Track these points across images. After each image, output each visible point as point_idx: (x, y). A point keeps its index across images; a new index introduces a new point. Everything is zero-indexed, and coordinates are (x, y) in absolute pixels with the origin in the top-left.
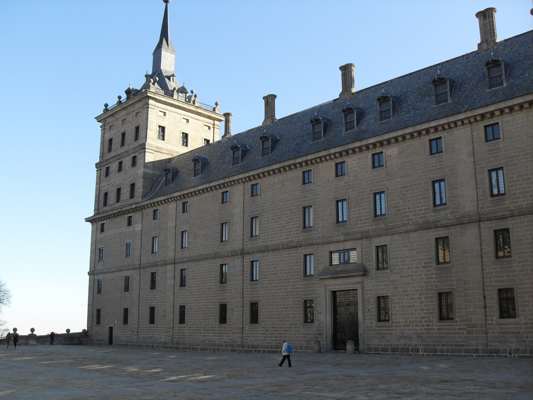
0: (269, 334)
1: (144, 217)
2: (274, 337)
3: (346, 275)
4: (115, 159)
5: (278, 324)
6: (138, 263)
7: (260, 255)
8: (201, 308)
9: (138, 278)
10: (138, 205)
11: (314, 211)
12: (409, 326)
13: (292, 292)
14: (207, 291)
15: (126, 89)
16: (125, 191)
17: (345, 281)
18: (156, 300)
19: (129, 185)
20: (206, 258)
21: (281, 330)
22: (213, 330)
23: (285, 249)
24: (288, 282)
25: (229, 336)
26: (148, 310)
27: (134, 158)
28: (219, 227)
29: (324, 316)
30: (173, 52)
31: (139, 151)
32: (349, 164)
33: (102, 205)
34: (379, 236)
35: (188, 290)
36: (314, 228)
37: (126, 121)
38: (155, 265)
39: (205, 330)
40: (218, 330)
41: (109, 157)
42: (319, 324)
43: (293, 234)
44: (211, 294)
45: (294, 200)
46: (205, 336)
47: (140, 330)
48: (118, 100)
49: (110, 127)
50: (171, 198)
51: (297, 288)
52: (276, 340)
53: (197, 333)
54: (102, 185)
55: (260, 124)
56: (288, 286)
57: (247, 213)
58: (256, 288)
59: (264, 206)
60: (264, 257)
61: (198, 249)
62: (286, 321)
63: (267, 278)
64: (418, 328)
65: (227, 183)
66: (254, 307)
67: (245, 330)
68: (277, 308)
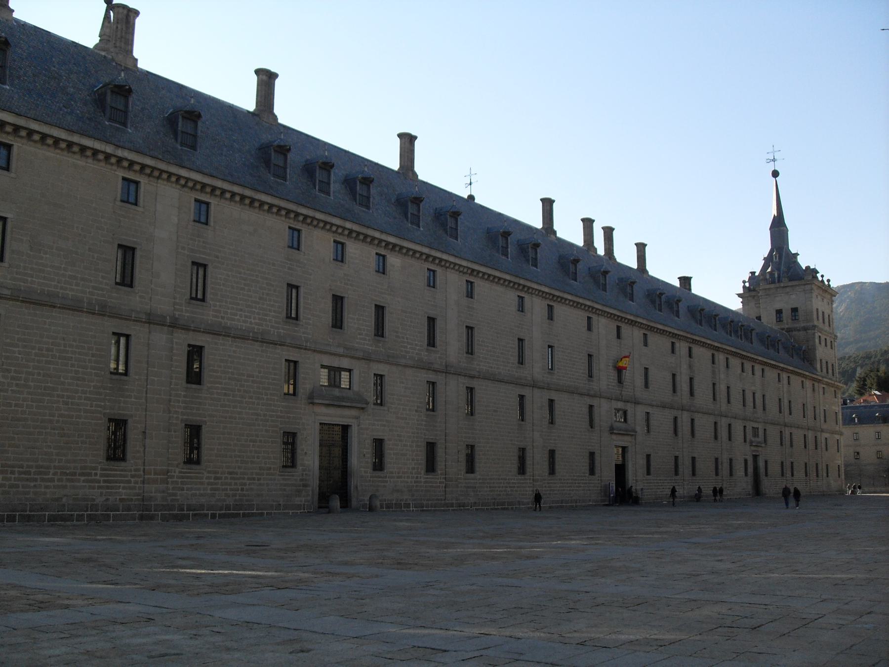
2: (231, 490)
3: (349, 404)
5: (239, 468)
12: (401, 477)
13: (265, 415)
17: (339, 411)
21: (244, 479)
22: (90, 474)
25: (134, 488)
29: (310, 457)
34: (379, 362)
35: (9, 371)
39: (63, 474)
40: (102, 475)
42: (304, 470)
46: (65, 487)
52: (235, 495)
53: (36, 480)
56: (258, 404)
63: (221, 383)
64: (409, 480)
66: (194, 432)
67: (173, 477)
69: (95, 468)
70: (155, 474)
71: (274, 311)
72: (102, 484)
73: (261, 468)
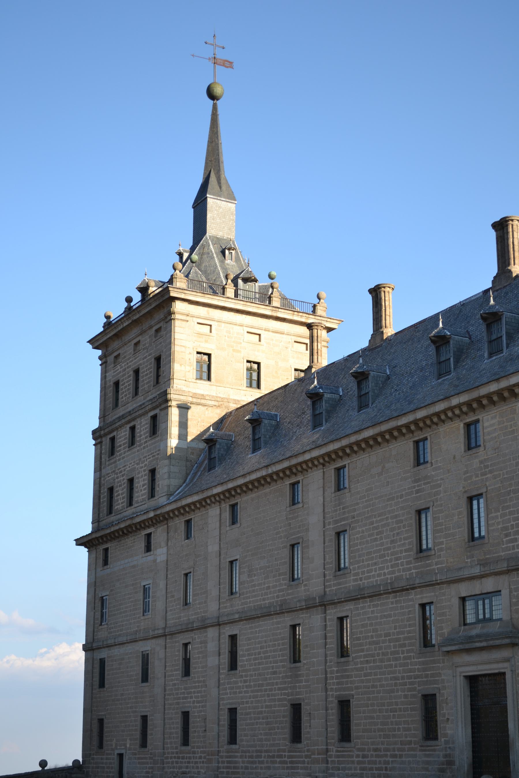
0: (369, 762)
1: (171, 533)
3: (484, 644)
4: (123, 421)
5: (383, 743)
6: (161, 624)
7: (350, 606)
8: (261, 712)
9: (162, 655)
10: (158, 512)
11: (434, 519)
13: (403, 678)
14: (270, 679)
15: (138, 284)
16: (142, 483)
17: (485, 656)
18: (191, 697)
19: (147, 472)
20: (267, 614)
21: (386, 756)
23: (390, 593)
24: (396, 659)
26: (178, 720)
27: (154, 418)
28: (286, 552)
30: (231, 197)
31: (160, 405)
32: (486, 424)
33: (105, 512)
35: (242, 676)
36: (433, 552)
37: (141, 346)
38: (189, 629)
39: (269, 757)
41: (114, 418)
42: (447, 742)
43: (402, 565)
44: (277, 684)
45: (402, 496)
46: (269, 768)
47: (167, 758)
48: (126, 304)
49: (116, 357)
50: (209, 497)
51: (410, 671)
54: (103, 471)
55: (364, 343)
57: (329, 523)
58: (346, 671)
59: (355, 510)
60: (357, 609)
61: (255, 596)
62: (394, 736)
63: (363, 651)
65: (295, 466)
67: (331, 756)
68: (380, 711)
69: (284, 751)
70: (318, 754)
71: (406, 551)
72: (289, 765)
73: (402, 743)
